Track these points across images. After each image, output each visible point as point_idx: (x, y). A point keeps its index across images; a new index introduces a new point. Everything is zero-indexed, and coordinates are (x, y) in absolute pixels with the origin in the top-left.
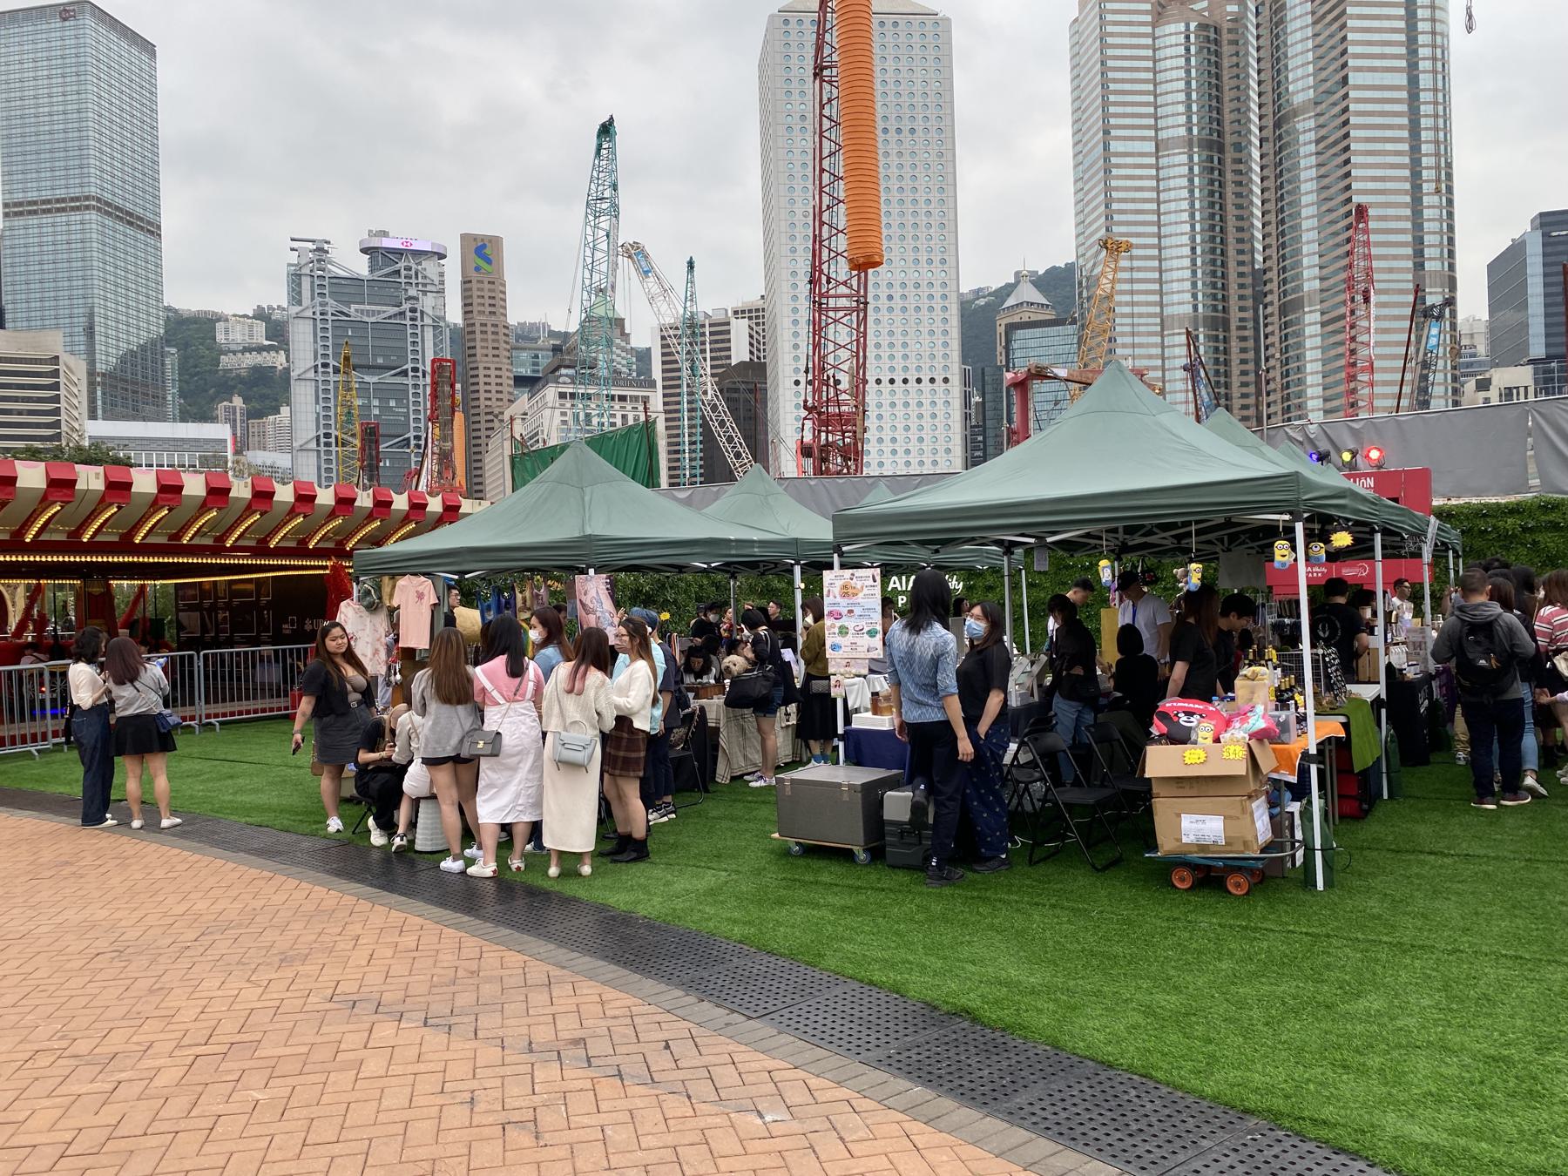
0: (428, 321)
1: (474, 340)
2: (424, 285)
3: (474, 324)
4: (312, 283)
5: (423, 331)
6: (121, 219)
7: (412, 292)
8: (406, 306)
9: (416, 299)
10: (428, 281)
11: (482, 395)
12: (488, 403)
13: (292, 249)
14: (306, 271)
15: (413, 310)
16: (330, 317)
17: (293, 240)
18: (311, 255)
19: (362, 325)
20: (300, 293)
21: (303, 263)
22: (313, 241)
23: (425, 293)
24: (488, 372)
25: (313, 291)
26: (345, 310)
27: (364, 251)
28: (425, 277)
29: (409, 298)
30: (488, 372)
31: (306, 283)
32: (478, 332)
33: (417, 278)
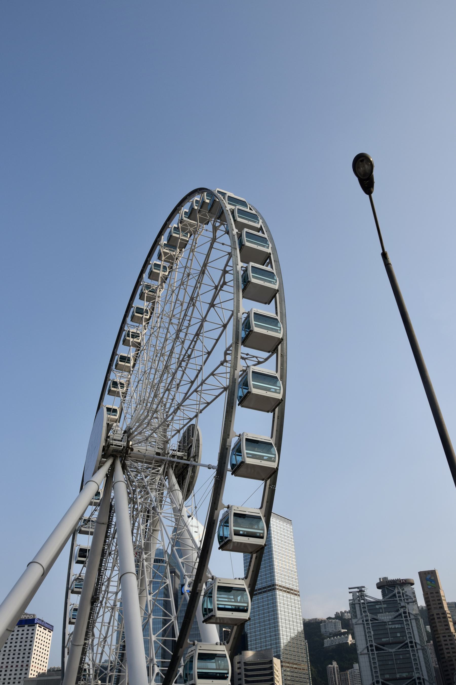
0: (412, 617)
1: (435, 623)
2: (407, 599)
3: (433, 615)
4: (360, 606)
5: (411, 623)
6: (285, 591)
7: (403, 604)
8: (402, 611)
9: (405, 607)
10: (408, 597)
11: (445, 651)
12: (449, 655)
13: (350, 593)
14: (356, 601)
15: (405, 613)
16: (370, 622)
17: (350, 589)
18: (358, 594)
19: (383, 624)
20: (355, 612)
21: (355, 598)
22: (358, 588)
23: (408, 603)
24: (445, 638)
25: (361, 610)
26: (375, 617)
27: (378, 588)
28: (407, 596)
29: (402, 607)
30: (445, 638)
31: (357, 607)
32: (436, 618)
33: (403, 597)
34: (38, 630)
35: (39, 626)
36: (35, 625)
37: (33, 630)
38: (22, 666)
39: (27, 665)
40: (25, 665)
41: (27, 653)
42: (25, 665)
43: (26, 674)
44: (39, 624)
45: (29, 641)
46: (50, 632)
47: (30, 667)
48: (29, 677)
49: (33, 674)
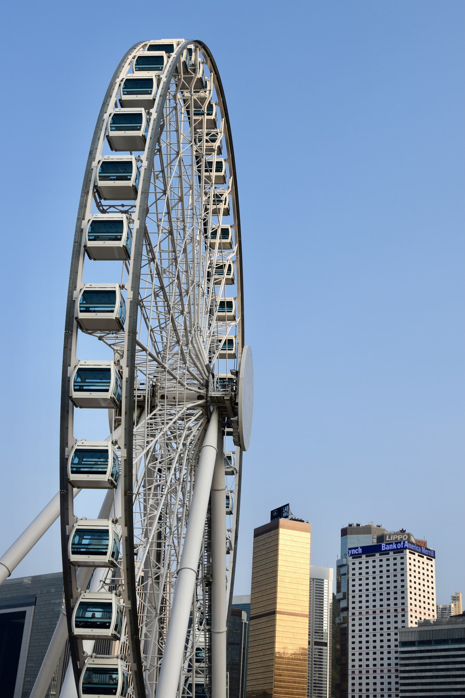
34: (410, 558)
35: (410, 552)
36: (404, 551)
37: (402, 558)
38: (396, 610)
39: (403, 610)
40: (399, 610)
41: (399, 589)
42: (399, 610)
43: (403, 622)
44: (409, 549)
45: (399, 575)
46: (431, 560)
47: (407, 612)
48: (409, 626)
49: (412, 623)
